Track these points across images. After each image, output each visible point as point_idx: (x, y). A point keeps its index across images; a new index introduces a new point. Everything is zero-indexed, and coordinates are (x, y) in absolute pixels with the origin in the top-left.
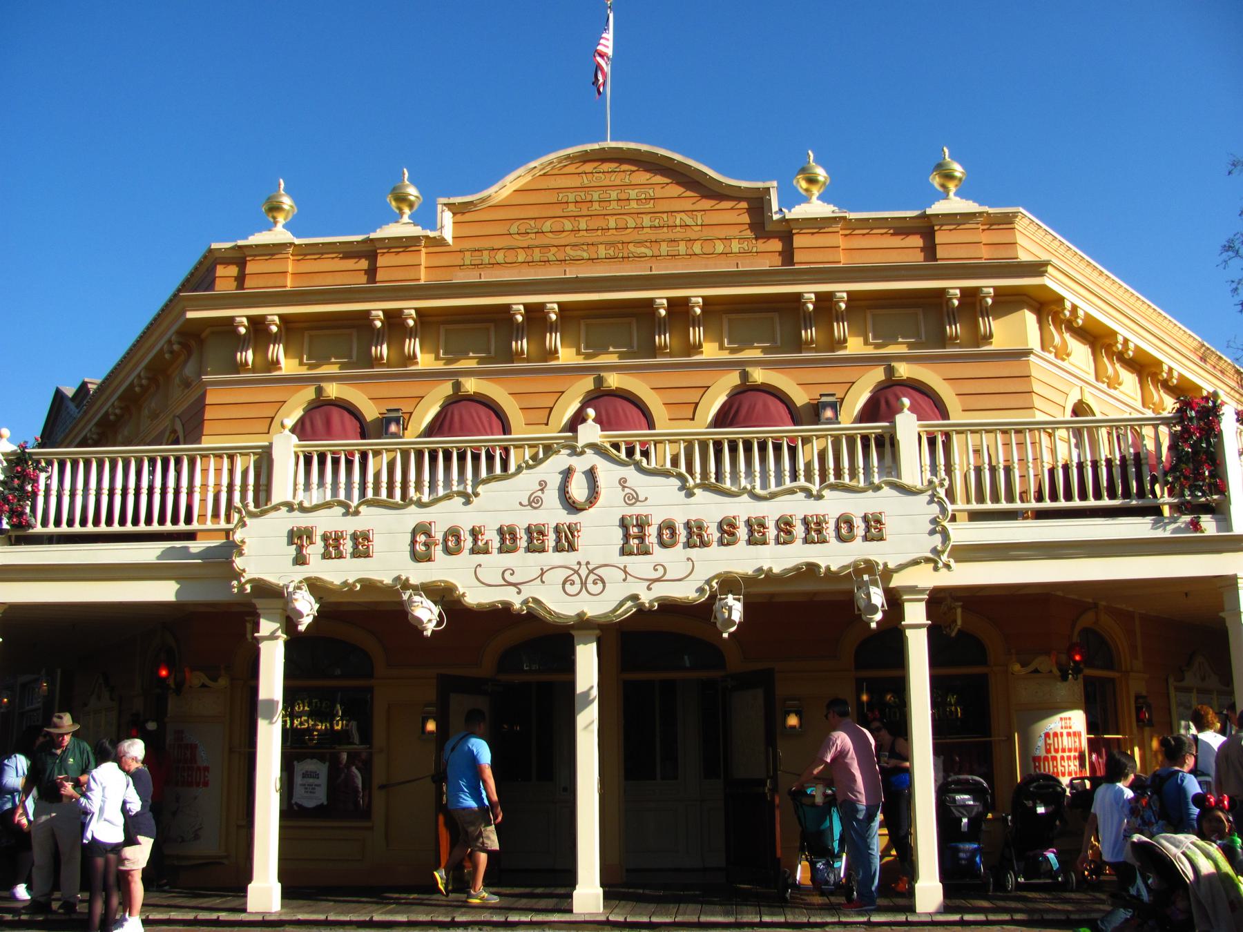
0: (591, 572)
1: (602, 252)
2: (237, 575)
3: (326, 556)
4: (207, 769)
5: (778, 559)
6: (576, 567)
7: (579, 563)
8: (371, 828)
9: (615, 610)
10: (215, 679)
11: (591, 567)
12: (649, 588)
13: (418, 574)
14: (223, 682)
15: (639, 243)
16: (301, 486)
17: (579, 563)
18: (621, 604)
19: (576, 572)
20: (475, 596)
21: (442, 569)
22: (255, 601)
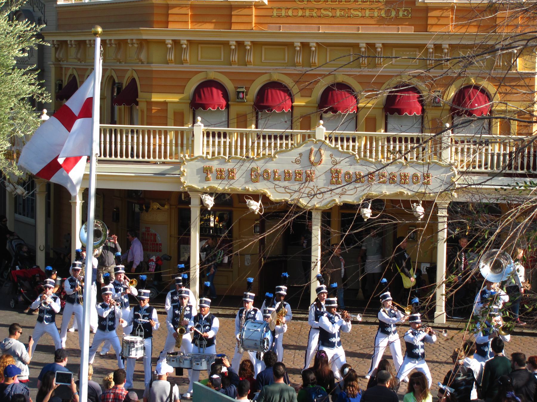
0: (318, 190)
1: (338, 13)
2: (182, 184)
3: (217, 178)
4: (160, 244)
5: (387, 191)
6: (313, 188)
7: (314, 186)
8: (232, 271)
9: (326, 205)
10: (163, 205)
11: (318, 188)
12: (340, 197)
13: (251, 188)
14: (166, 207)
15: (355, 10)
16: (205, 146)
17: (314, 186)
18: (329, 202)
19: (313, 189)
20: (273, 197)
21: (263, 187)
22: (189, 193)
